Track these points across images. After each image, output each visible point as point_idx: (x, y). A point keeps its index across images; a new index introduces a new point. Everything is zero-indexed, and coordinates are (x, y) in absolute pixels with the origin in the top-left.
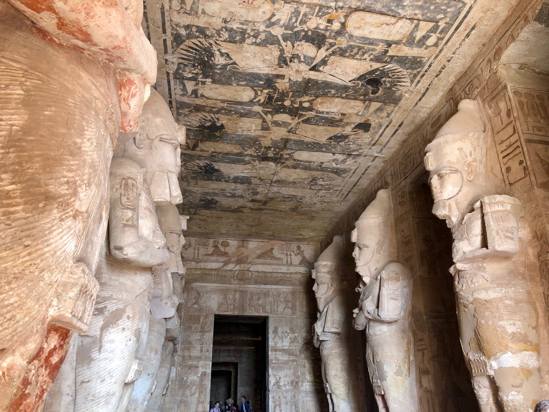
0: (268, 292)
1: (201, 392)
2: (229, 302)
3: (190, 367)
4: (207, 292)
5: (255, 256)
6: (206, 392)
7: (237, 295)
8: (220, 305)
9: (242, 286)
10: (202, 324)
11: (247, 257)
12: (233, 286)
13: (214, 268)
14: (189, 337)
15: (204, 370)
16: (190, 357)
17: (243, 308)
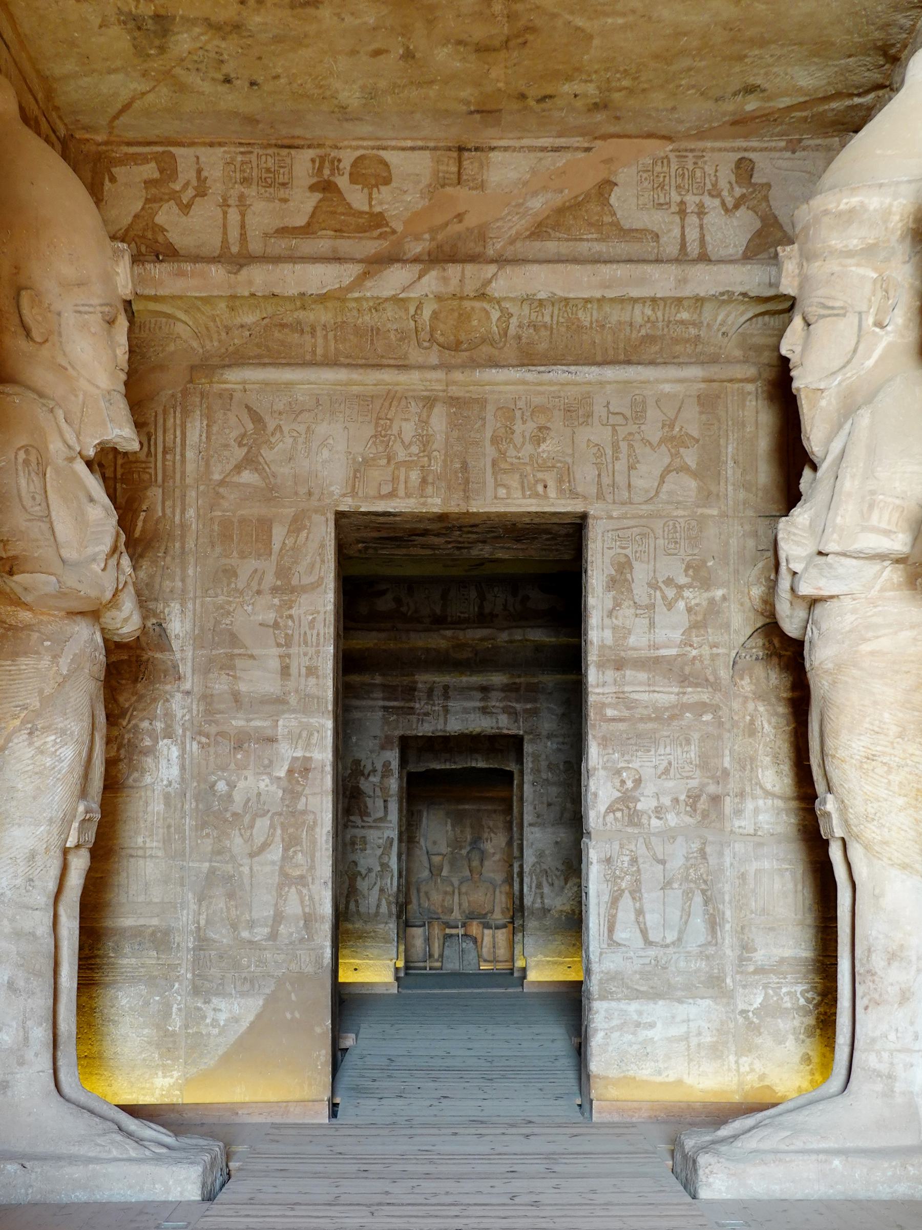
0: (586, 399)
1: (290, 843)
2: (402, 455)
3: (240, 742)
4: (295, 411)
5: (519, 224)
6: (314, 842)
7: (439, 421)
8: (358, 471)
9: (458, 376)
10: (281, 555)
11: (482, 234)
12: (415, 376)
13: (313, 289)
14: (229, 613)
15: (299, 754)
16: (236, 697)
17: (464, 478)
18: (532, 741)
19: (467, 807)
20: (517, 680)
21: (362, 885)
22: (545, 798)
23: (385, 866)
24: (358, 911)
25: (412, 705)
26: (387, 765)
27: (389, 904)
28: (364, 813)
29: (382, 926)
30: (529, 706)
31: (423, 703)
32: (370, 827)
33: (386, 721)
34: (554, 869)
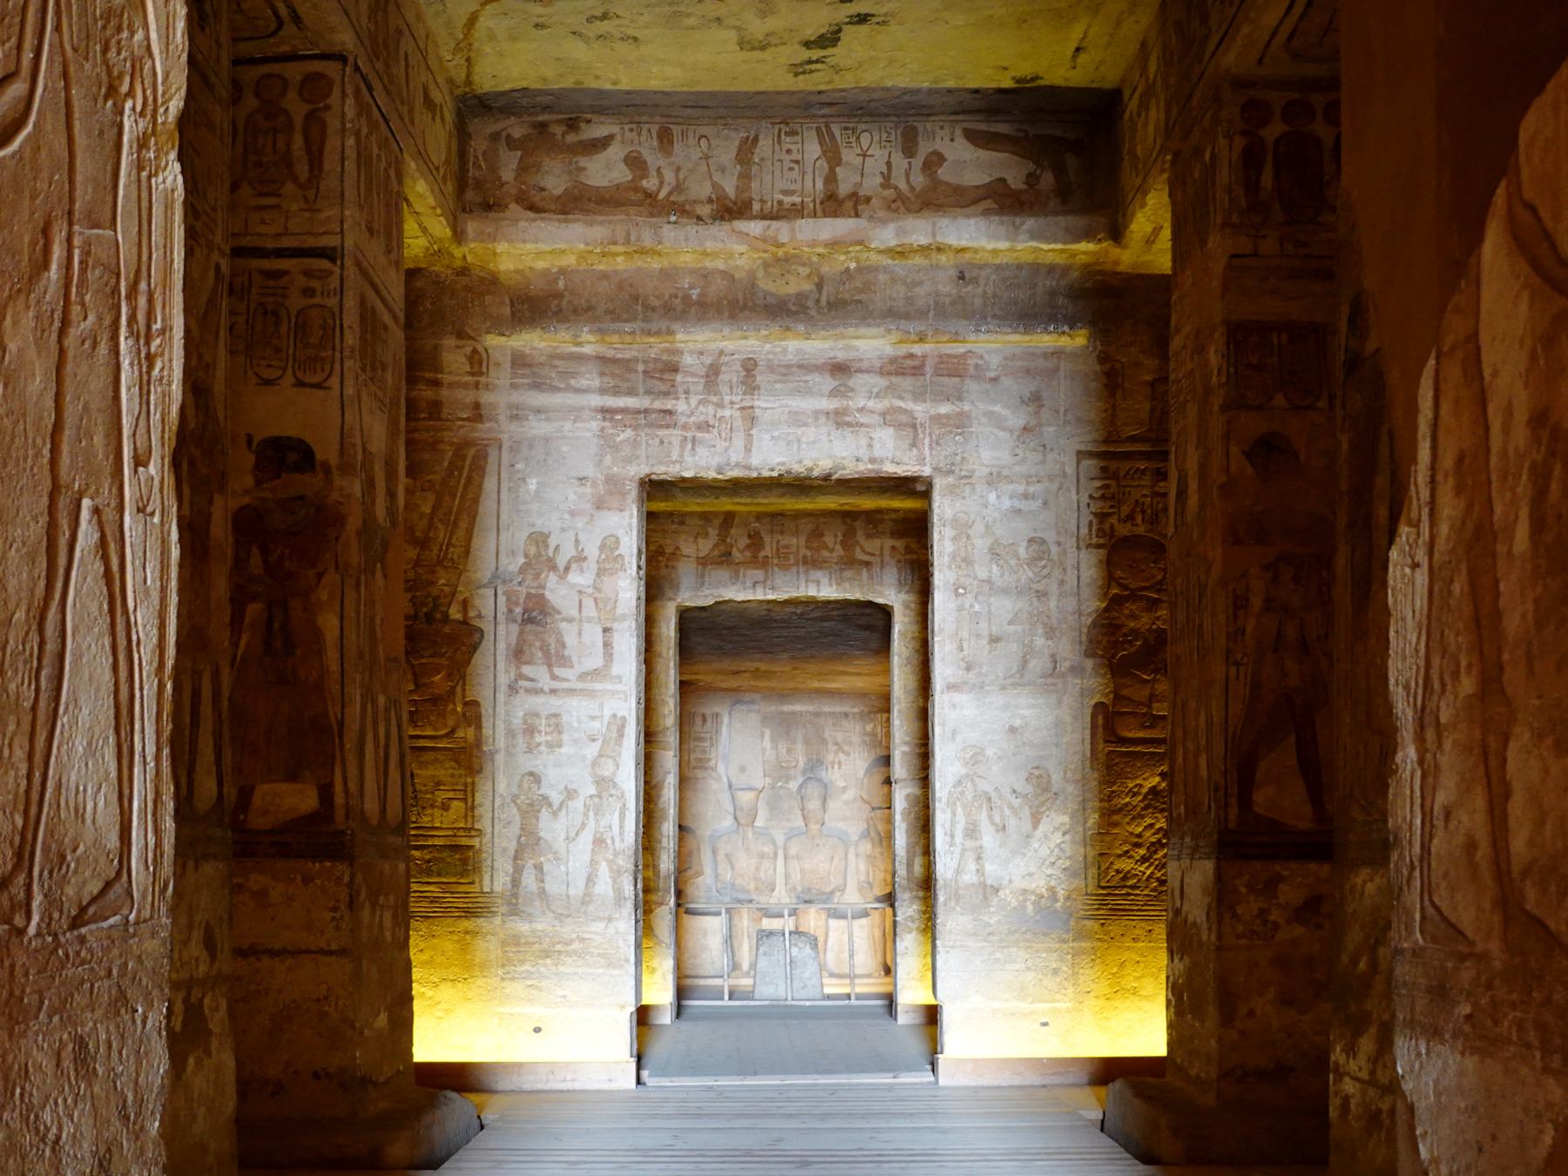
18: (951, 491)
19: (797, 708)
20: (917, 349)
21: (552, 829)
22: (984, 626)
23: (604, 784)
24: (542, 893)
25: (668, 404)
26: (609, 545)
27: (616, 874)
28: (555, 658)
29: (599, 927)
30: (944, 409)
31: (694, 401)
32: (572, 692)
33: (608, 444)
34: (1006, 792)
